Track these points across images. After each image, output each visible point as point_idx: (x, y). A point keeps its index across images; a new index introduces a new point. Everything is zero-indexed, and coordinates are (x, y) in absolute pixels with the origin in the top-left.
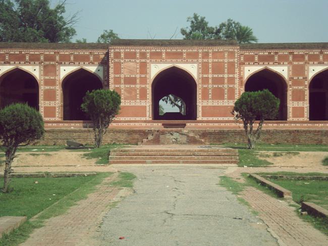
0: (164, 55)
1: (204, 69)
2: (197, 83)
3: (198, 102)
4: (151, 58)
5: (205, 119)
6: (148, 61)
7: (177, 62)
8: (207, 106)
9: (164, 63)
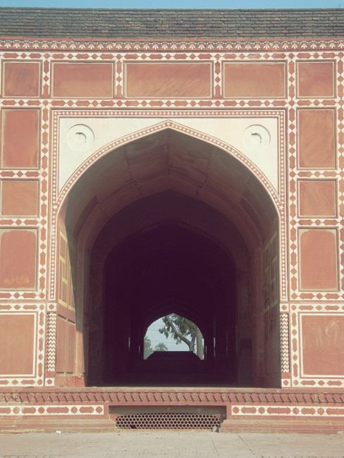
0: (120, 79)
1: (314, 138)
2: (279, 208)
3: (283, 298)
4: (58, 90)
5: (322, 382)
6: (45, 105)
7: (183, 111)
8: (330, 318)
9: (129, 111)
